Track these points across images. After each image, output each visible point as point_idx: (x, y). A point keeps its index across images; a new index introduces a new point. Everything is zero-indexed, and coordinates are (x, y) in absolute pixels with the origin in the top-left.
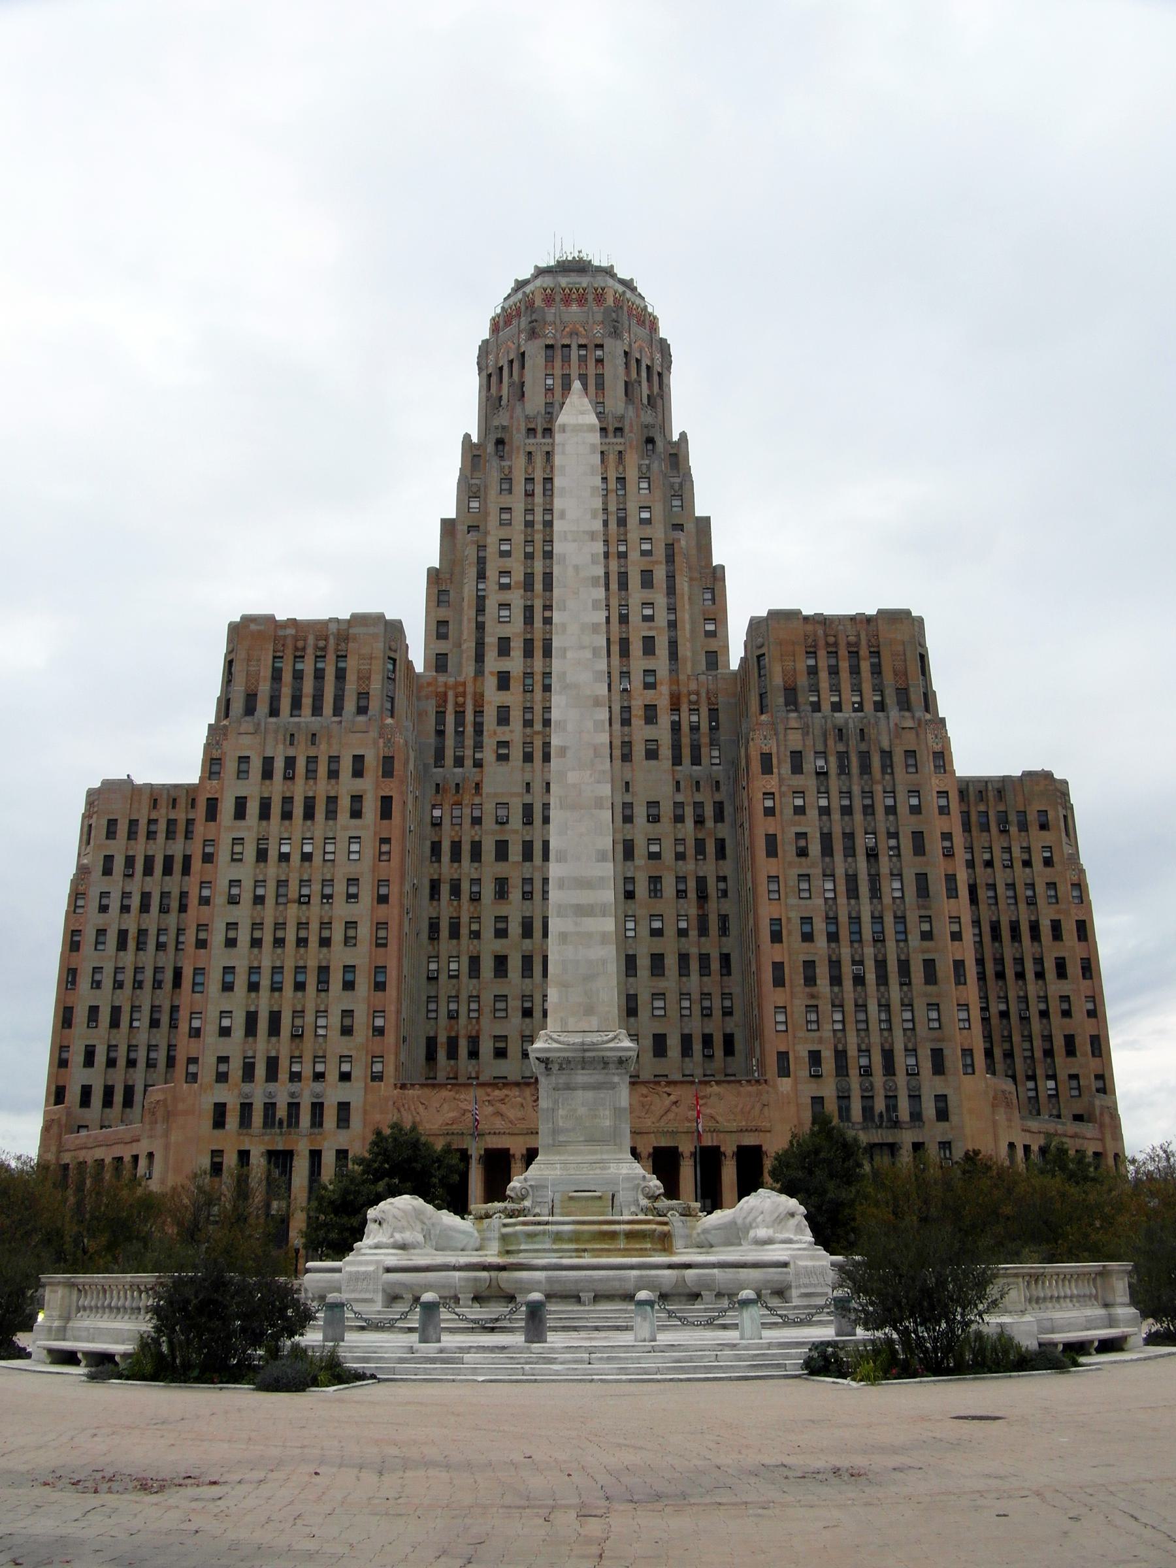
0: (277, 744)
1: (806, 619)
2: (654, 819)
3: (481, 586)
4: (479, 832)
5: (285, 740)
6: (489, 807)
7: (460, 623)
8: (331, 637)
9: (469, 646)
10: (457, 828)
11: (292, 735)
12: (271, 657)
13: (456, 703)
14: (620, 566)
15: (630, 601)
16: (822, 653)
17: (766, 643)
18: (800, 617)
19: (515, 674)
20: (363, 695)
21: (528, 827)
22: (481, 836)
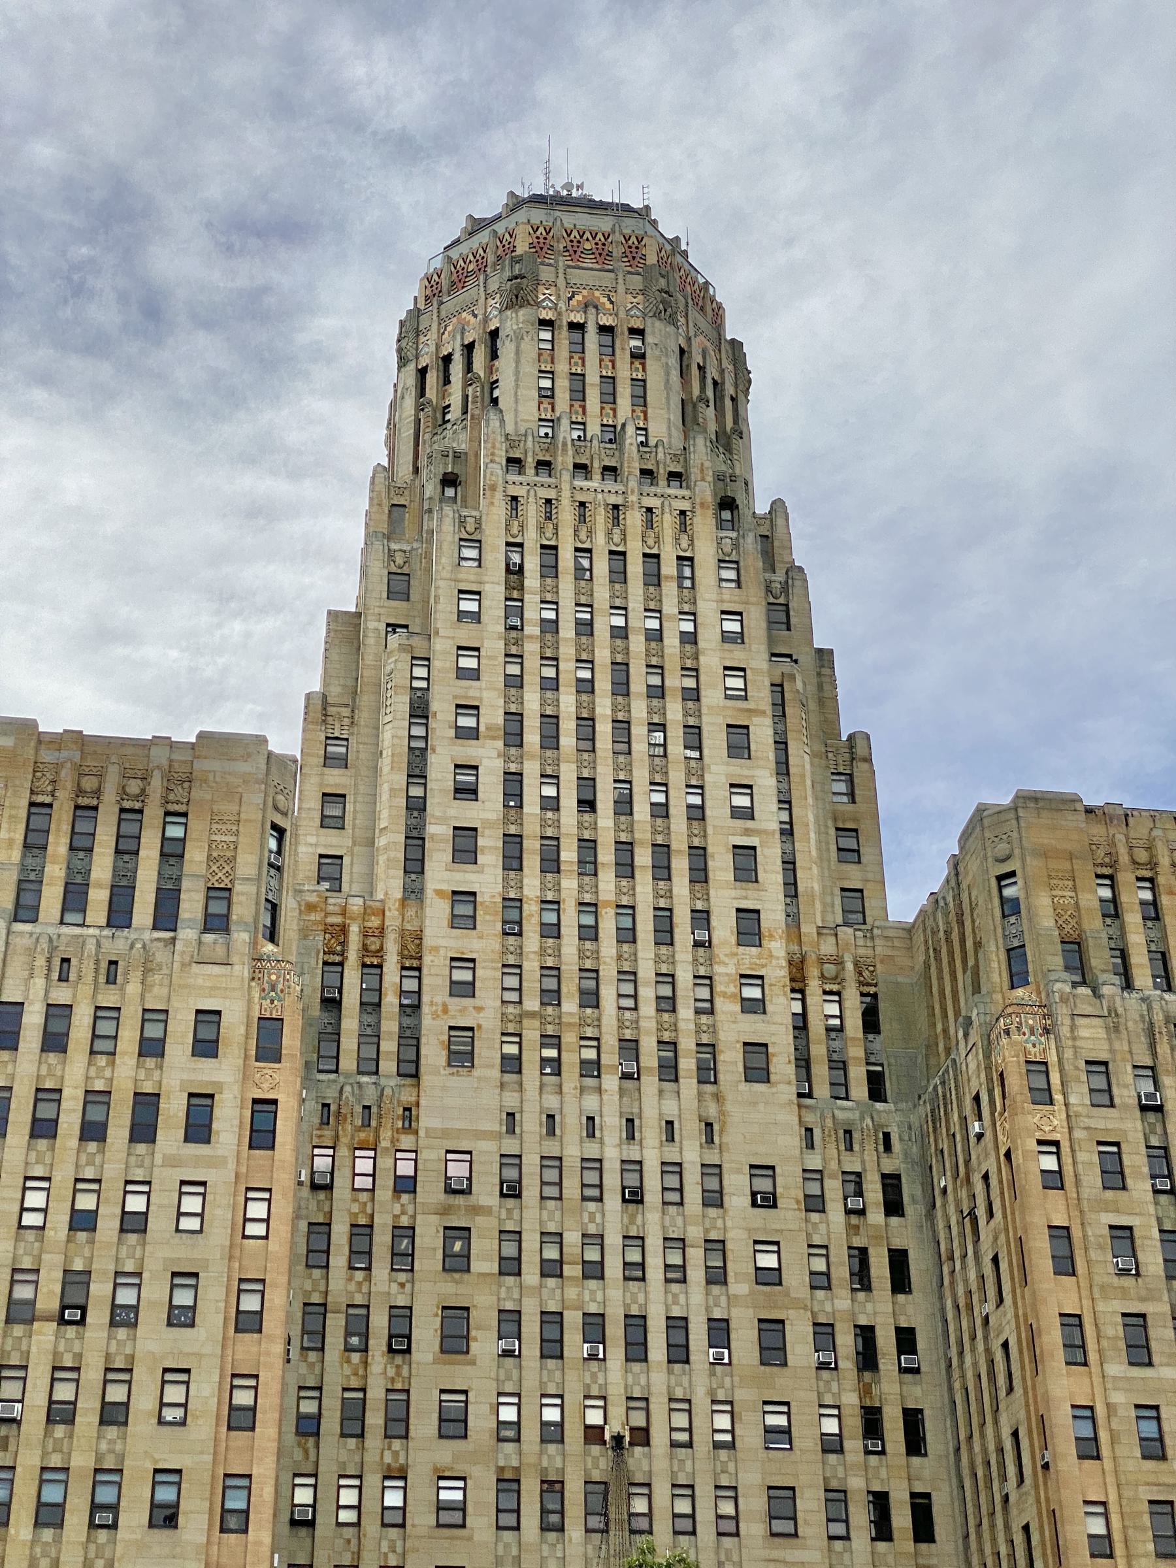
0: (31, 976)
1: (1089, 811)
2: (765, 1201)
3: (418, 731)
4: (410, 1209)
5: (49, 969)
6: (431, 1155)
7: (373, 797)
8: (157, 774)
9: (391, 841)
10: (364, 1197)
11: (66, 961)
12: (25, 803)
13: (365, 948)
14: (686, 714)
15: (707, 777)
16: (1126, 878)
17: (1017, 851)
18: (1079, 807)
19: (487, 898)
20: (219, 893)
21: (511, 1203)
22: (414, 1217)
